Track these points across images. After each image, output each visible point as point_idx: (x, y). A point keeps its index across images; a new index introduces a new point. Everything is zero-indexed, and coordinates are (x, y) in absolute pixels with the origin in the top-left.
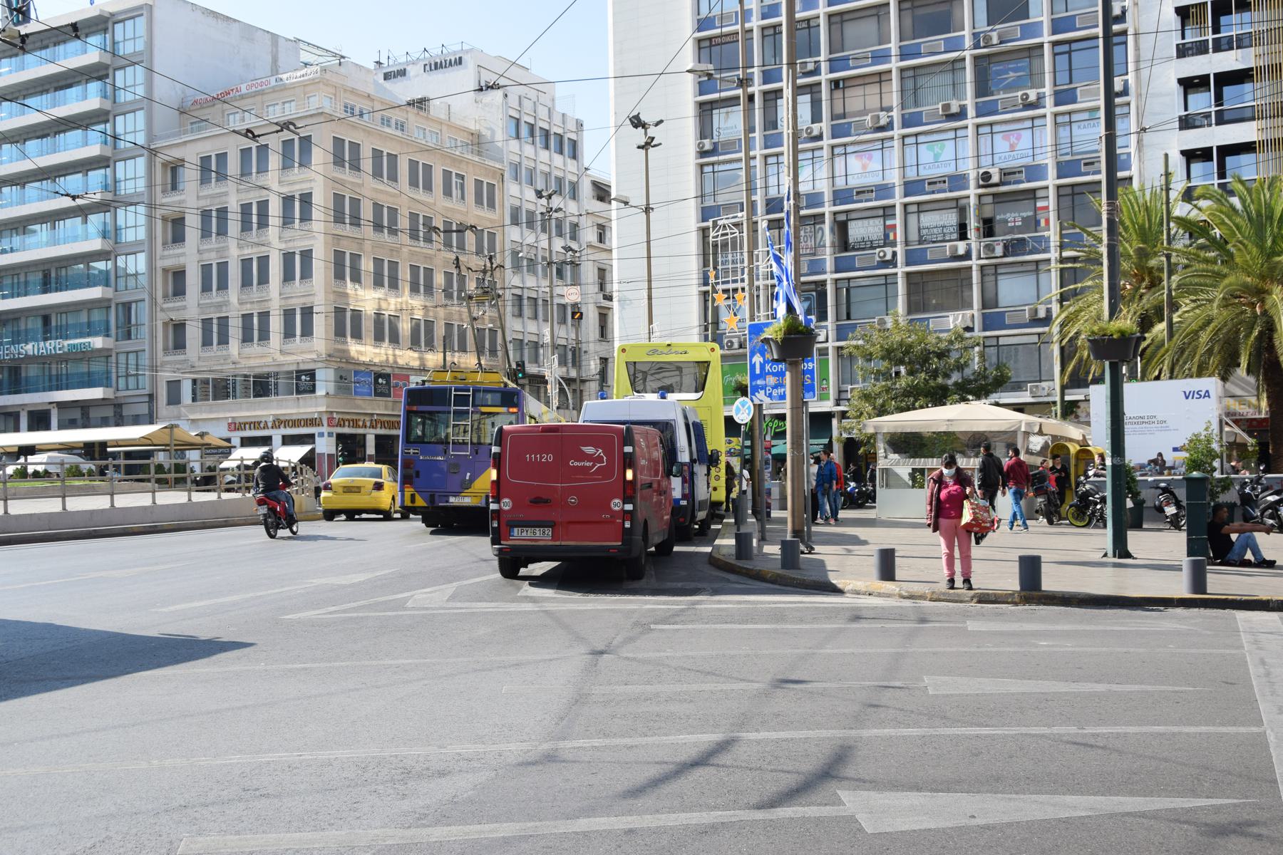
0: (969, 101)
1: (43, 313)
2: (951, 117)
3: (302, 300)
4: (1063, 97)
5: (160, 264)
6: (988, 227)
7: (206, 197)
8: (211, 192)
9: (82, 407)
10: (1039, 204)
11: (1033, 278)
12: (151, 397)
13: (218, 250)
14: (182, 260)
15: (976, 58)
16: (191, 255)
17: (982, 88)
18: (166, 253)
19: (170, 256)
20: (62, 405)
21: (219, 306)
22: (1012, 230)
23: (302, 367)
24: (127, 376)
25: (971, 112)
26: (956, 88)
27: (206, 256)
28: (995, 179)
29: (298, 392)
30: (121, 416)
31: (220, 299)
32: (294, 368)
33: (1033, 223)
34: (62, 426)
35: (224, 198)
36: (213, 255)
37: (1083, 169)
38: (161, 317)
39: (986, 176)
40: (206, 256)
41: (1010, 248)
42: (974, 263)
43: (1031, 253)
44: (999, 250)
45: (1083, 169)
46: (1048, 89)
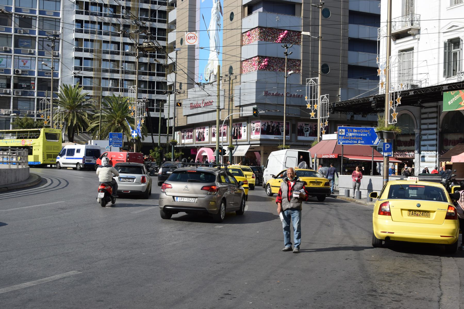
0: (12, 48)
2: (6, 51)
4: (41, 53)
6: (16, 86)
10: (32, 82)
11: (29, 102)
15: (15, 35)
17: (16, 46)
22: (22, 88)
25: (13, 52)
26: (9, 44)
28: (20, 73)
33: (29, 87)
37: (45, 74)
39: (17, 71)
41: (24, 93)
42: (12, 96)
43: (29, 96)
44: (20, 94)
45: (45, 74)
46: (36, 50)
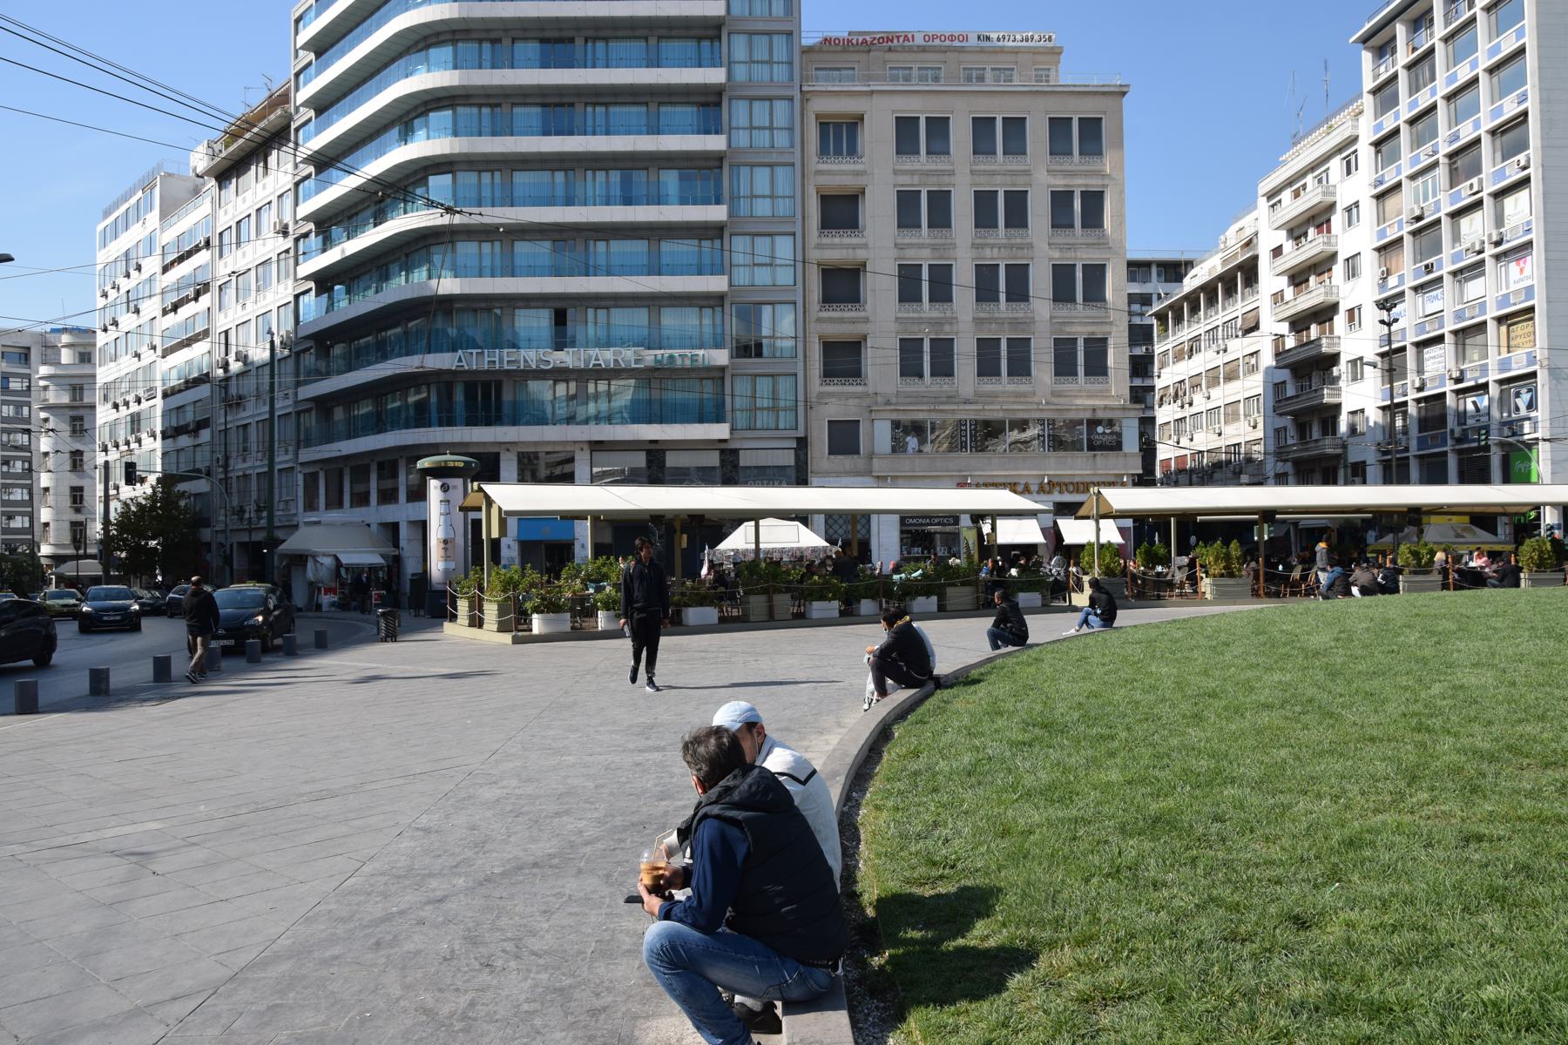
1: (559, 305)
3: (1090, 329)
5: (815, 255)
7: (912, 173)
8: (917, 166)
9: (649, 452)
12: (802, 443)
13: (934, 248)
14: (861, 255)
16: (964, 249)
18: (825, 240)
19: (832, 246)
20: (597, 446)
21: (937, 323)
23: (1100, 415)
24: (753, 409)
27: (910, 253)
29: (1091, 448)
30: (736, 466)
31: (936, 314)
32: (1088, 415)
34: (595, 479)
35: (946, 179)
36: (926, 253)
38: (816, 331)
40: (910, 253)
